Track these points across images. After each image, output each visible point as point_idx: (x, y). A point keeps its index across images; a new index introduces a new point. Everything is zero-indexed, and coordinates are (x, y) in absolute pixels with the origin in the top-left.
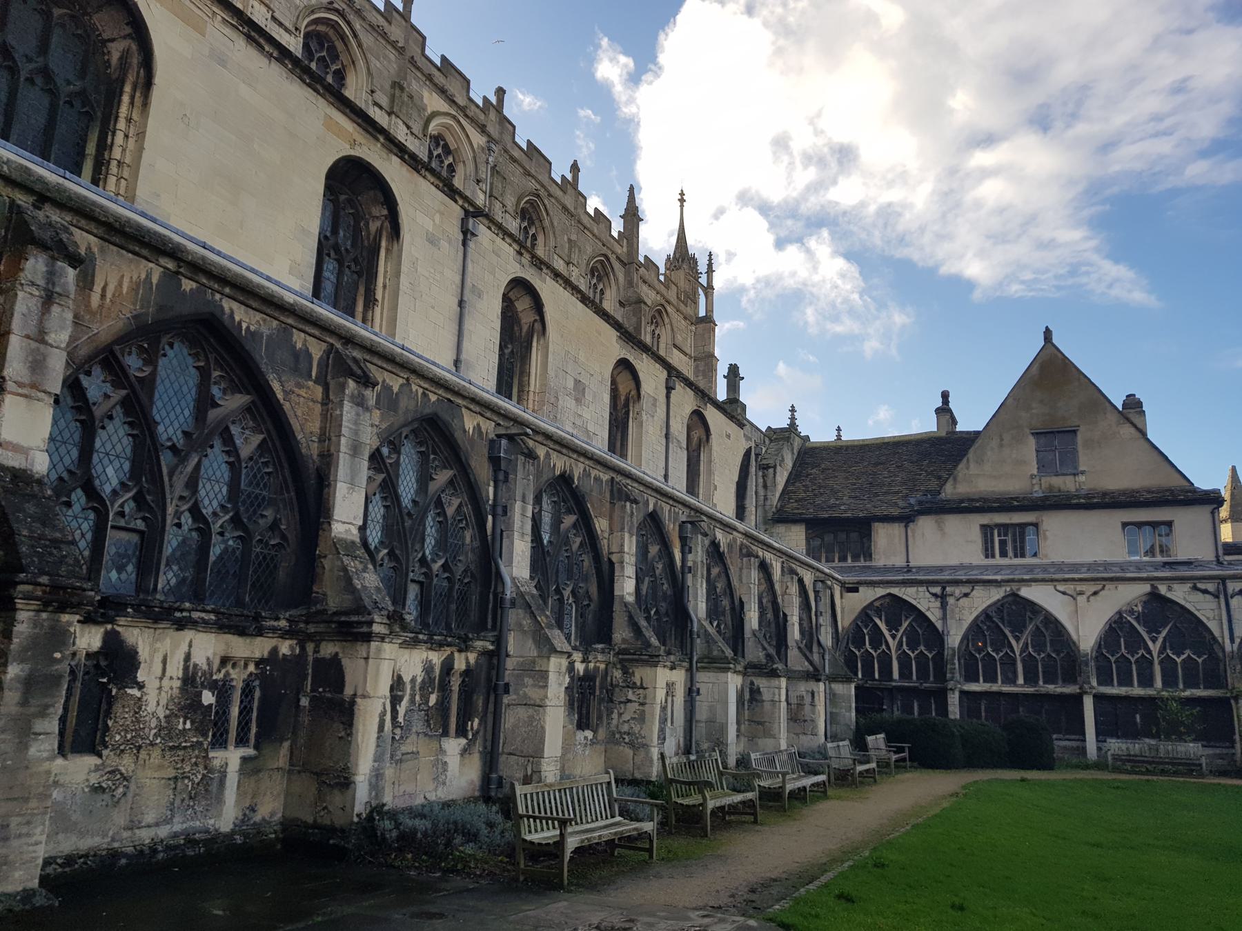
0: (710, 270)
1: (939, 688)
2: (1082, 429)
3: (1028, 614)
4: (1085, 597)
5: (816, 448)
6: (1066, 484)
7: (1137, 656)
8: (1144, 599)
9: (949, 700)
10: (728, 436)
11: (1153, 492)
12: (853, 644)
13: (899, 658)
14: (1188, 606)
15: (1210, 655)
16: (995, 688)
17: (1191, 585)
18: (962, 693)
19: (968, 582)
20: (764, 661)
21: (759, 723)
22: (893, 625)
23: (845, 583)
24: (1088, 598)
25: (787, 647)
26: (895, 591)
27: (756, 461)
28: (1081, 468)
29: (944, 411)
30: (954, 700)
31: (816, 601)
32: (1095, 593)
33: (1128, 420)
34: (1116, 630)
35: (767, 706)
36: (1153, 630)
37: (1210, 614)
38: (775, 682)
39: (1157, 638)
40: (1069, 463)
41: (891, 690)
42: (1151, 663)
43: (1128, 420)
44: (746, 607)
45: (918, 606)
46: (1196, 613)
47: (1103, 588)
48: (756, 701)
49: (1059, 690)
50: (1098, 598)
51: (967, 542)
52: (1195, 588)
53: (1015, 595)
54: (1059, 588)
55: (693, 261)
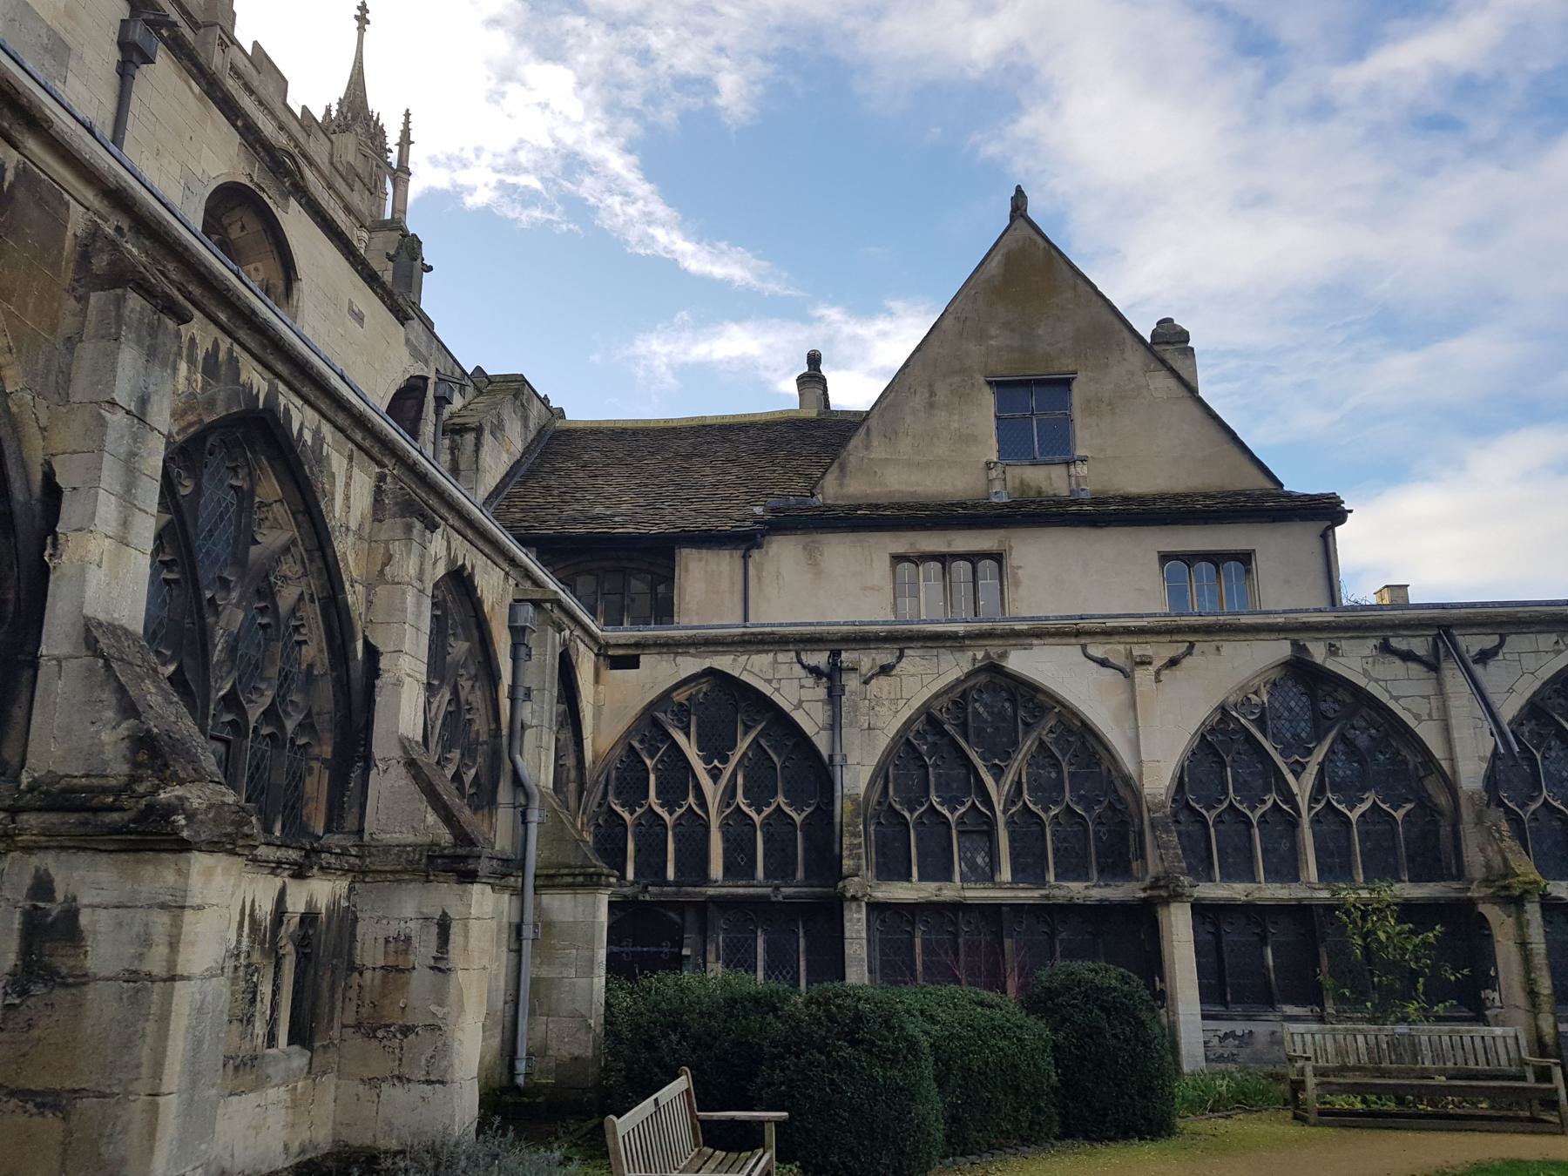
0: (405, 140)
1: (814, 896)
3: (1021, 713)
4: (1152, 669)
5: (576, 431)
6: (1051, 480)
8: (1275, 675)
9: (847, 925)
10: (359, 318)
11: (1213, 497)
12: (618, 795)
13: (724, 826)
14: (1373, 689)
15: (1421, 804)
16: (949, 892)
18: (876, 908)
19: (890, 638)
20: (119, 769)
21: (52, 1102)
22: (715, 749)
23: (608, 645)
24: (1158, 673)
25: (368, 760)
26: (724, 662)
27: (438, 413)
28: (1080, 452)
29: (812, 379)
30: (856, 924)
31: (515, 658)
32: (1173, 662)
33: (1163, 362)
35: (102, 1002)
37: (1422, 708)
38: (159, 876)
39: (1303, 766)
40: (1059, 448)
41: (703, 908)
42: (1293, 823)
43: (1163, 362)
44: (70, 512)
45: (777, 698)
46: (1392, 705)
48: (53, 978)
50: (1178, 673)
51: (865, 589)
52: (1386, 648)
53: (993, 669)
54: (1094, 651)
55: (377, 133)
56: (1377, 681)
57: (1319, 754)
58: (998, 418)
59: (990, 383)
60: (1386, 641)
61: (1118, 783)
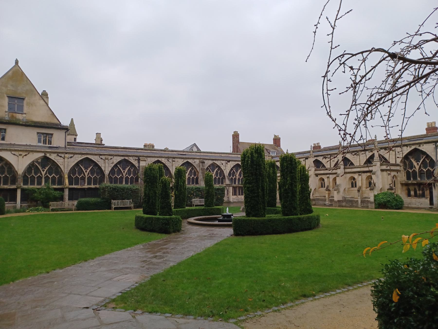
2: (26, 98)
4: (22, 156)
7: (37, 176)
8: (42, 158)
14: (55, 161)
15: (60, 176)
17: (57, 154)
28: (25, 112)
32: (26, 155)
33: (43, 98)
34: (31, 167)
36: (44, 167)
39: (44, 170)
40: (21, 110)
42: (41, 178)
43: (43, 98)
47: (28, 154)
49: (9, 187)
52: (58, 155)
56: (56, 159)
57: (47, 169)
58: (9, 103)
59: (7, 96)
60: (58, 154)
61: (15, 172)
